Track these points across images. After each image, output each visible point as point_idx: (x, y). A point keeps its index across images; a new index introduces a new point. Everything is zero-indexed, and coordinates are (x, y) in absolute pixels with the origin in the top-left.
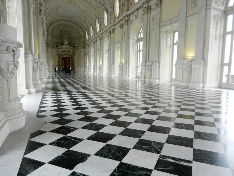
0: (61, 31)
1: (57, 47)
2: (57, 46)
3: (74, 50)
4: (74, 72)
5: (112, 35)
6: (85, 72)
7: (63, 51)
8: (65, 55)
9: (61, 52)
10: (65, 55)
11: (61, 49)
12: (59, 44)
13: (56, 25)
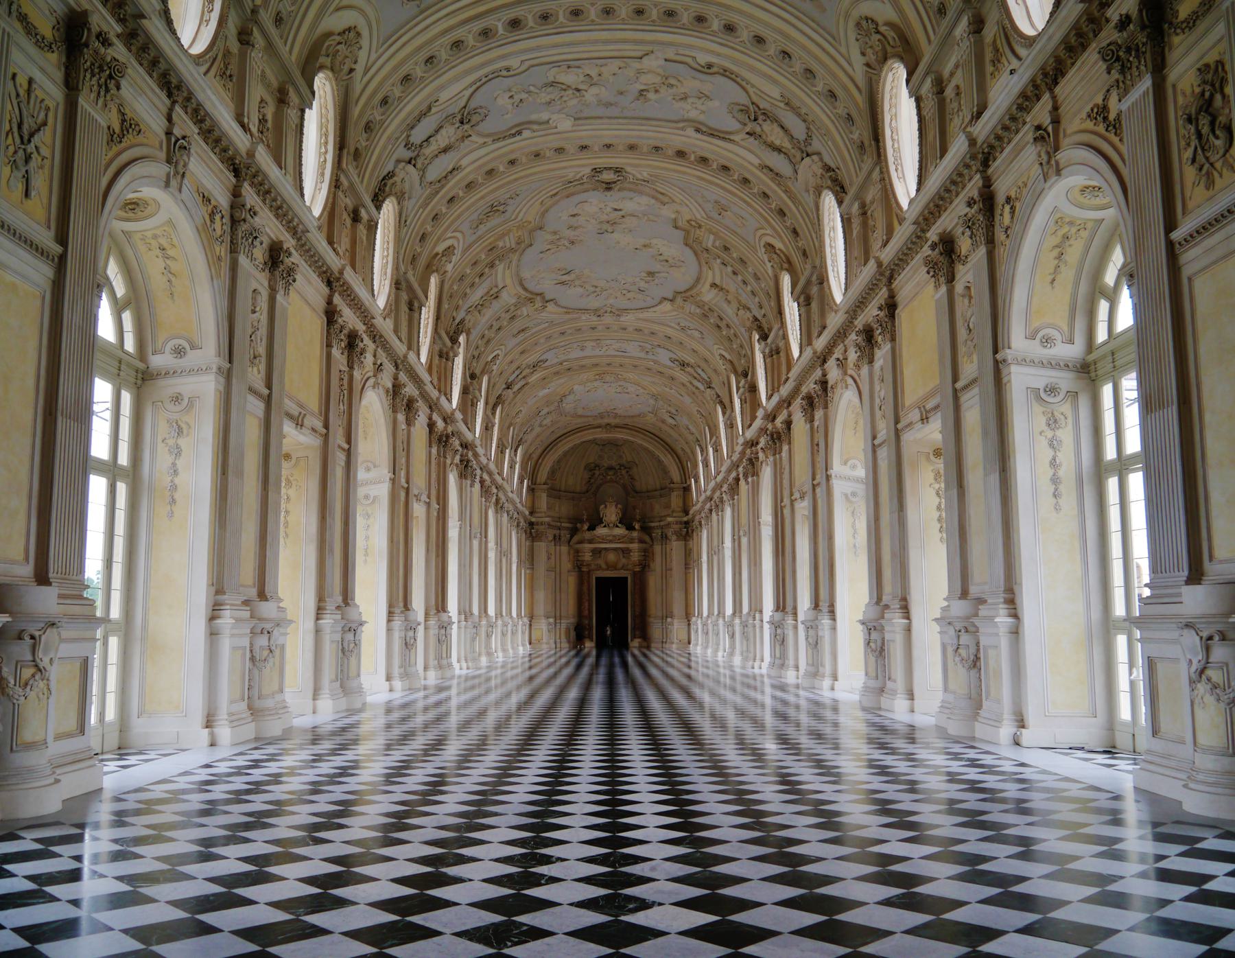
0: (591, 468)
1: (572, 537)
2: (574, 531)
3: (644, 545)
4: (645, 644)
5: (882, 354)
6: (689, 643)
7: (597, 552)
9: (587, 557)
11: (590, 542)
12: (582, 522)
13: (566, 448)
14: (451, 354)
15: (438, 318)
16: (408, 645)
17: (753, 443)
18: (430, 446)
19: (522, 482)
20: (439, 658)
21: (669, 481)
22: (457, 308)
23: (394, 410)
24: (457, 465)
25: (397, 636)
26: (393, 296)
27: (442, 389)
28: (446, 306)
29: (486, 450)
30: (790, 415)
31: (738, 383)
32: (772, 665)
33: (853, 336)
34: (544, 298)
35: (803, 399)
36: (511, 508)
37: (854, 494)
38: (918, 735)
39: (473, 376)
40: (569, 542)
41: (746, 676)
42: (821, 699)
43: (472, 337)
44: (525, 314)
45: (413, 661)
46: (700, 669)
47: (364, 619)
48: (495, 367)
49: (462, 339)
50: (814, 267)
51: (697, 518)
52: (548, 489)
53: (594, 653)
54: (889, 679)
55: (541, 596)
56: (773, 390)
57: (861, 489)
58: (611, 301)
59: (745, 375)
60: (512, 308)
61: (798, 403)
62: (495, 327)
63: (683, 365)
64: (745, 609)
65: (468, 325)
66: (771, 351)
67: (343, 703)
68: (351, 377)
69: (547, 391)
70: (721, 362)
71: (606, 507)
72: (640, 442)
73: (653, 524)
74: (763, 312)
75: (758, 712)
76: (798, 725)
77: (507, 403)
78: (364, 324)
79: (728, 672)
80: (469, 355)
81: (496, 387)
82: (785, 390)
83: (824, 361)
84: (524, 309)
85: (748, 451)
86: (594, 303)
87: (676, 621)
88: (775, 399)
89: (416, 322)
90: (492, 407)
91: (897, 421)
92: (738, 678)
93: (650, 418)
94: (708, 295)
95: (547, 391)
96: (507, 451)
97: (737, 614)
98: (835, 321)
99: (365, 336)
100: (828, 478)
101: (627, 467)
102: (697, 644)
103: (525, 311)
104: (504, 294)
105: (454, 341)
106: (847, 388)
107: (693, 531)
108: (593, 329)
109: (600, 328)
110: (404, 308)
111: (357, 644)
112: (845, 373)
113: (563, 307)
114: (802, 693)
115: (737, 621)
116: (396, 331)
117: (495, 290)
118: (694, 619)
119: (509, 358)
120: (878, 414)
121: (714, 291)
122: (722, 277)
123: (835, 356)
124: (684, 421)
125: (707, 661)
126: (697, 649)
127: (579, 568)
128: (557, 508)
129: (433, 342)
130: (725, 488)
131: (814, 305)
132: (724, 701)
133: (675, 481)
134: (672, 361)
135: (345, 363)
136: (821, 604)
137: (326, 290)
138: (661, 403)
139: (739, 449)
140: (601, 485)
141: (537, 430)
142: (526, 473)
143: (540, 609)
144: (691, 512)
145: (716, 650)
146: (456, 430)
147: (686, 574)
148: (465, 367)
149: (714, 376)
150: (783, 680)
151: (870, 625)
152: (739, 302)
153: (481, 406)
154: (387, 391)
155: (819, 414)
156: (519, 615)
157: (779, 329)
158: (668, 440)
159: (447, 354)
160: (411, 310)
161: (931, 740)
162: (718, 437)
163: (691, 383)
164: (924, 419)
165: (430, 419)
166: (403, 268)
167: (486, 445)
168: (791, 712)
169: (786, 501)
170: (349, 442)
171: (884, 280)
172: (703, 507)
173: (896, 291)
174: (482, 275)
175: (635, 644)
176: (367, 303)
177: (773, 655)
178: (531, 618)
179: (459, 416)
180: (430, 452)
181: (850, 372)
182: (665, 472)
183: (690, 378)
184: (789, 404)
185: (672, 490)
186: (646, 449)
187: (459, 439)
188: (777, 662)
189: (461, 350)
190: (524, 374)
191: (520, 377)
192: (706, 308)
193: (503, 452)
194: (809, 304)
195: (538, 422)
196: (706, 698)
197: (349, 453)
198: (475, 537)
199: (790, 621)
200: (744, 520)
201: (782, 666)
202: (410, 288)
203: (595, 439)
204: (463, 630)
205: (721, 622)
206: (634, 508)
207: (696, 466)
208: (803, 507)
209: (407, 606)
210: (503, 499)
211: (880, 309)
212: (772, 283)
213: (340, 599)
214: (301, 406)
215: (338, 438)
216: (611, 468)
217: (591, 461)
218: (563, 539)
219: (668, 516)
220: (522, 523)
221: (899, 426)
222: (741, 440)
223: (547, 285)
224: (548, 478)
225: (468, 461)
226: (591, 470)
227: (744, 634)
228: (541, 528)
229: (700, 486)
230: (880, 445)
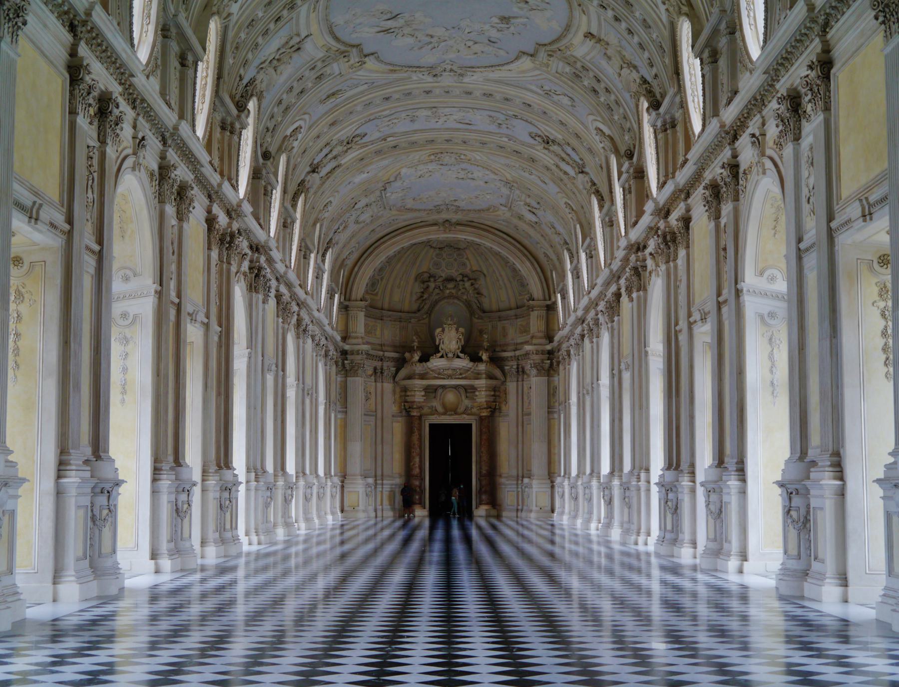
0: (425, 279)
1: (398, 371)
2: (401, 363)
4: (494, 512)
6: (553, 511)
8: (447, 411)
10: (447, 411)
11: (423, 377)
12: (411, 350)
13: (391, 252)
14: (237, 126)
15: (219, 77)
16: (180, 512)
17: (639, 247)
18: (209, 248)
19: (332, 297)
20: (221, 528)
21: (527, 297)
22: (245, 63)
23: (161, 198)
24: (245, 274)
25: (165, 499)
26: (159, 46)
27: (226, 172)
28: (231, 61)
29: (284, 254)
30: (688, 210)
31: (620, 166)
32: (661, 540)
33: (774, 105)
34: (361, 51)
35: (706, 188)
36: (317, 331)
37: (772, 315)
38: (852, 632)
39: (266, 155)
40: (394, 377)
41: (627, 554)
42: (726, 585)
43: (265, 103)
44: (337, 72)
45: (186, 535)
46: (567, 545)
47: (120, 478)
48: (296, 144)
49: (252, 105)
50: (724, 11)
51: (564, 346)
52: (366, 306)
53: (427, 523)
54: (816, 558)
55: (356, 448)
56: (666, 176)
57: (781, 308)
58: (452, 56)
59: (630, 156)
60: (319, 64)
61: (699, 193)
62: (296, 91)
63: (547, 142)
64: (627, 467)
65: (260, 86)
66: (664, 125)
67: (94, 588)
68: (103, 155)
69: (364, 176)
70: (597, 138)
71: (443, 331)
72: (488, 244)
73: (505, 354)
74: (654, 71)
75: (642, 601)
76: (695, 618)
77: (312, 191)
78: (120, 84)
79: (603, 550)
80: (261, 128)
81: (298, 172)
82: (683, 176)
83: (735, 138)
84: (335, 65)
85: (633, 258)
86: (429, 58)
87: (535, 483)
88: (670, 188)
89: (190, 82)
90: (292, 197)
91: (830, 218)
92: (617, 557)
93: (504, 213)
94: (581, 49)
95: (366, 175)
96: (313, 256)
97: (616, 473)
98: (749, 84)
99: (120, 100)
100: (738, 293)
101: (472, 278)
102: (562, 513)
103: (335, 68)
104: (308, 46)
105: (241, 107)
106: (764, 173)
107: (558, 363)
108: (428, 92)
109: (437, 91)
110: (174, 63)
111: (112, 510)
112: (763, 154)
113: (386, 64)
114: (700, 576)
115: (616, 482)
116: (163, 94)
117: (296, 40)
118: (558, 480)
119: (314, 132)
120: (806, 208)
121: (590, 43)
122: (600, 25)
123: (750, 131)
124: (548, 217)
125: (576, 535)
126: (563, 519)
127: (408, 412)
128: (378, 332)
129: (213, 108)
130: (602, 306)
131: (723, 63)
132: (597, 587)
133: (535, 296)
134: (533, 136)
135: (95, 135)
136: (726, 460)
137: (68, 37)
138: (518, 192)
139: (620, 254)
140: (436, 302)
141: (353, 227)
142: (337, 285)
143: (356, 465)
144: (556, 339)
145: (588, 521)
146: (243, 226)
147: (549, 419)
148: (255, 142)
149: (587, 157)
150: (675, 560)
151: (792, 488)
152: (623, 58)
153: (277, 195)
154: (152, 175)
155: (727, 208)
156: (327, 473)
157: (675, 95)
158: (526, 242)
159: (232, 125)
160: (183, 65)
161: (869, 639)
162: (593, 239)
163: (557, 166)
164: (867, 215)
165: (209, 211)
166: (172, 9)
167: (284, 249)
168: (686, 602)
169: (683, 325)
170: (100, 241)
171: (817, 29)
172: (572, 333)
173: (832, 43)
174: (278, 19)
175: (480, 512)
176: (124, 56)
177: (663, 528)
178: (344, 477)
179: (247, 208)
180: (209, 257)
181: (769, 152)
182: (523, 284)
183: (557, 160)
184: (688, 195)
185: (531, 308)
186: (497, 254)
187: (248, 239)
188: (668, 536)
189: (251, 120)
190: (334, 153)
191: (330, 156)
192: (579, 65)
193: (306, 257)
194: (715, 61)
195: (353, 218)
196: (575, 583)
197: (100, 258)
198: (269, 370)
199: (685, 482)
200: (626, 349)
201: (675, 541)
202: (182, 36)
203: (429, 241)
204: (253, 493)
205: (594, 483)
206: (481, 332)
207: (563, 277)
208: (704, 333)
209: (178, 460)
210: (306, 319)
211: (810, 67)
212: (666, 33)
213: (88, 451)
214: (36, 194)
215: (86, 236)
216: (450, 279)
217: (424, 268)
219: (526, 343)
220: (332, 352)
221: (834, 225)
222: (623, 243)
223: (366, 34)
224: (367, 292)
225: (260, 269)
226: (423, 282)
227: (626, 501)
228: (358, 358)
229: (569, 303)
230: (807, 250)
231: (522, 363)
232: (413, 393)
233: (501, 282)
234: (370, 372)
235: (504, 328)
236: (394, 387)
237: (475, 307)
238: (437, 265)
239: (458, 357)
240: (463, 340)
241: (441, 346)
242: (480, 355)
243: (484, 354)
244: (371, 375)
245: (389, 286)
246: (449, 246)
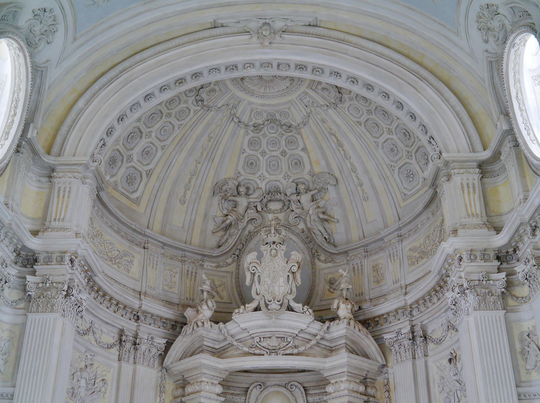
1: (169, 345)
128: (135, 269)
217: (228, 172)
218: (143, 347)
231: (419, 318)
232: (198, 388)
233: (367, 187)
234: (110, 338)
235: (376, 269)
236: (163, 378)
237: (320, 240)
238: (251, 164)
239: (290, 309)
240: (298, 276)
241: (256, 287)
242: (335, 306)
243: (342, 306)
244: (110, 347)
245: (164, 195)
246: (272, 120)
